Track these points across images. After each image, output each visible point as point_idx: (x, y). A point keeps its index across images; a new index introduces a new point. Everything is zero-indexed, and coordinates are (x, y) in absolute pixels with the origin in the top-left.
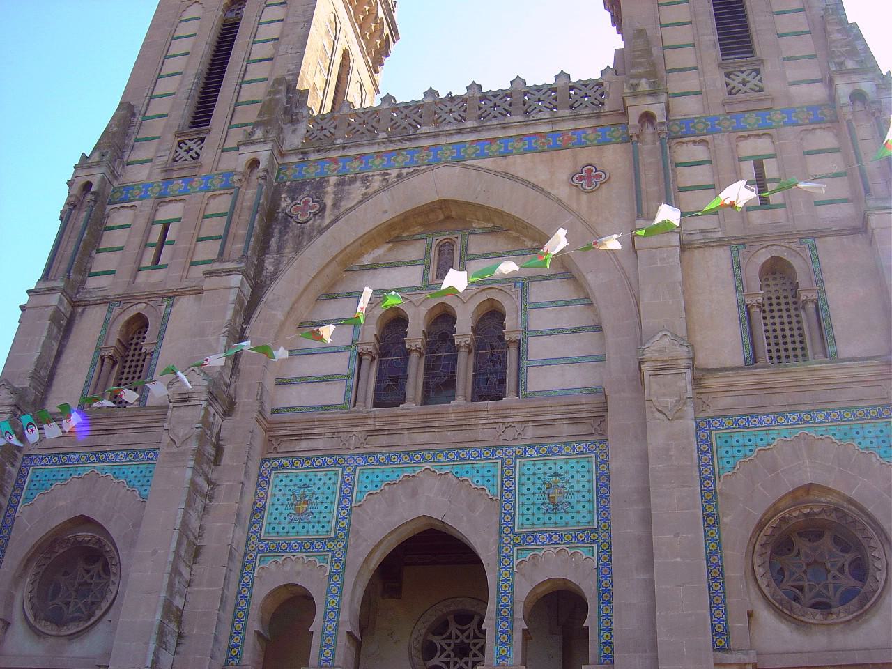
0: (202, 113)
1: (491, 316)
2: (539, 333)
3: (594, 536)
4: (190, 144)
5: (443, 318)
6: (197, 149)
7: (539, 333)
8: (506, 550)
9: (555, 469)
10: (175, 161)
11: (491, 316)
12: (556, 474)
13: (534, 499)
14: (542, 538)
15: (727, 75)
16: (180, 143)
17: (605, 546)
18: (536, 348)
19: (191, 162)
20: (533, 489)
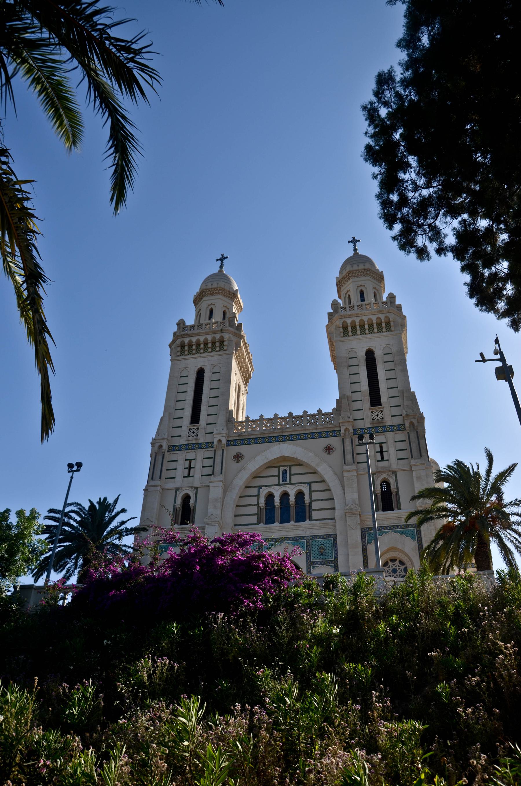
0: (195, 418)
1: (300, 495)
2: (315, 501)
3: (333, 562)
4: (194, 430)
5: (285, 495)
6: (196, 432)
7: (315, 501)
8: (309, 567)
9: (322, 543)
10: (189, 437)
11: (300, 495)
12: (322, 544)
13: (316, 552)
14: (319, 563)
15: (372, 412)
16: (190, 429)
17: (336, 565)
18: (315, 505)
19: (195, 437)
20: (316, 549)
